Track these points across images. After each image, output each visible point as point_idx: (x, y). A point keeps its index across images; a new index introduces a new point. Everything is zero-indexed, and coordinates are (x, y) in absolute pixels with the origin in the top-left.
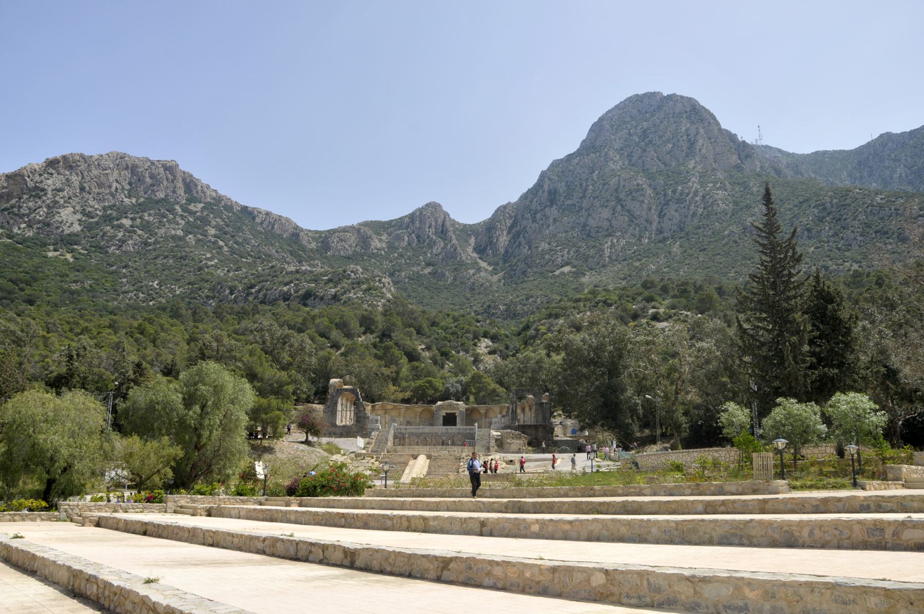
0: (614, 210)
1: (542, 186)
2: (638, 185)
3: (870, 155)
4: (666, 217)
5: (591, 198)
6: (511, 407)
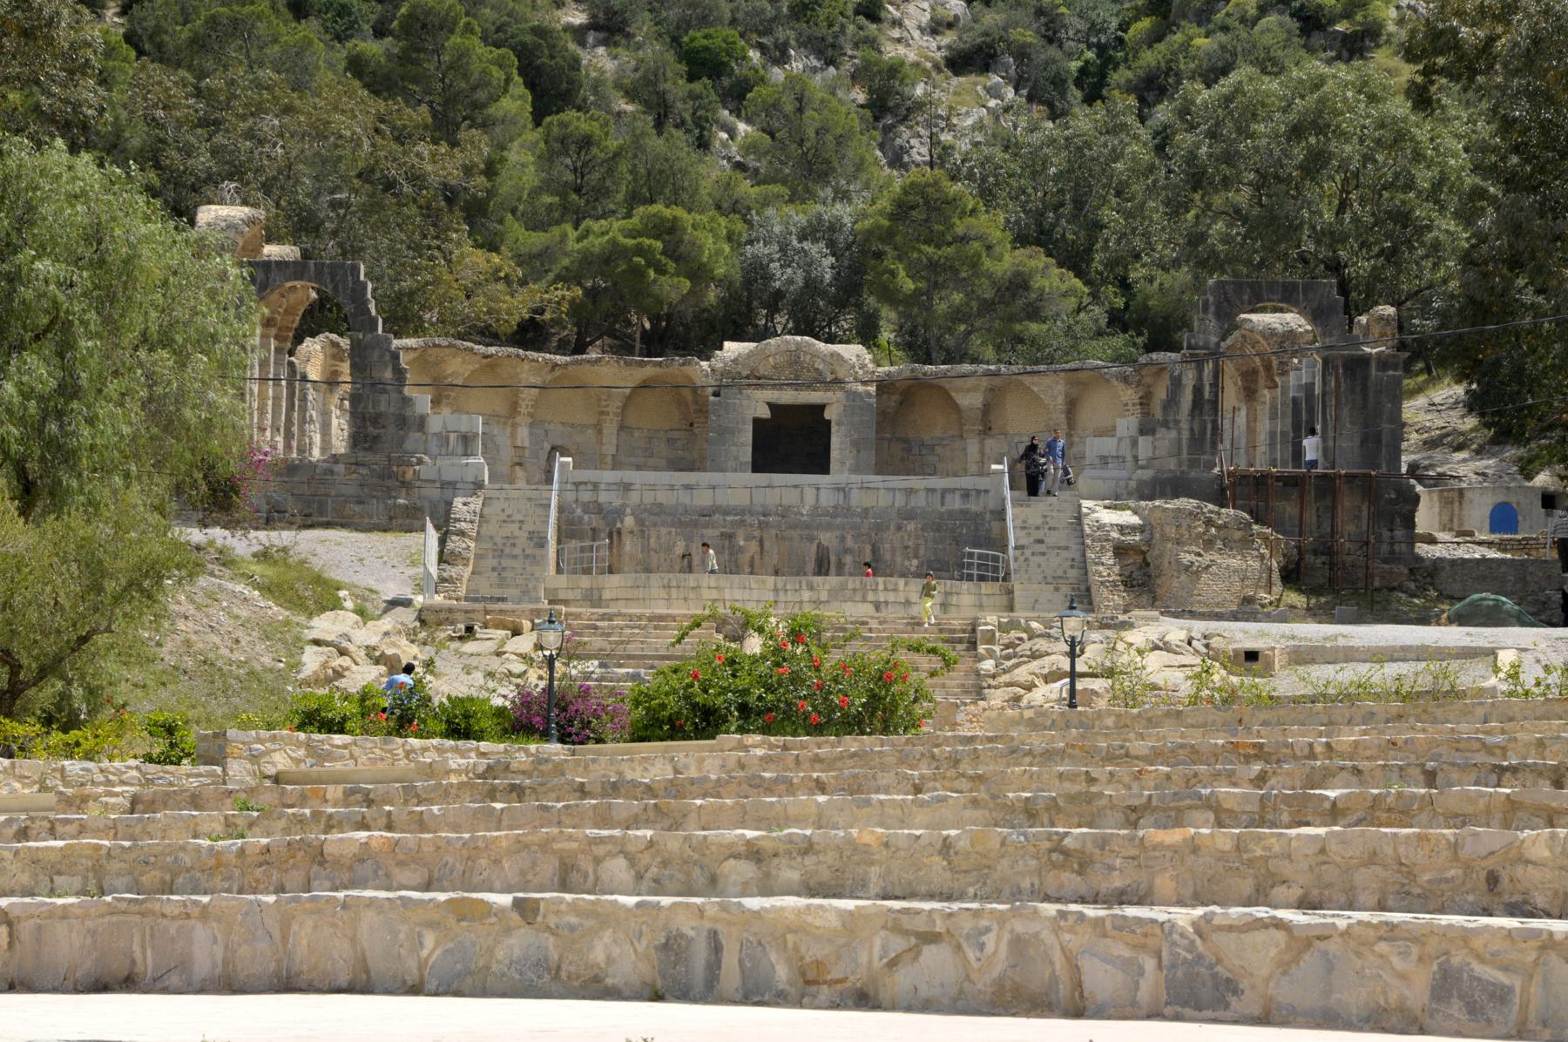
6: (1189, 379)
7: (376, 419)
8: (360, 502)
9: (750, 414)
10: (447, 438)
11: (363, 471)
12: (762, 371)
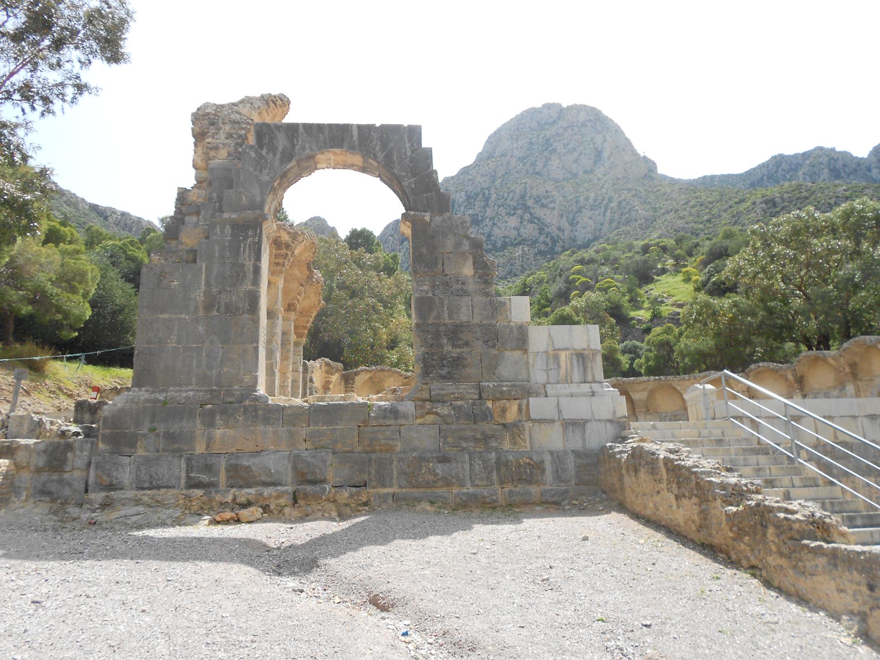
0: (521, 218)
2: (547, 192)
3: (764, 175)
4: (579, 225)
5: (496, 207)
7: (455, 333)
8: (444, 460)
10: (556, 358)
11: (444, 410)
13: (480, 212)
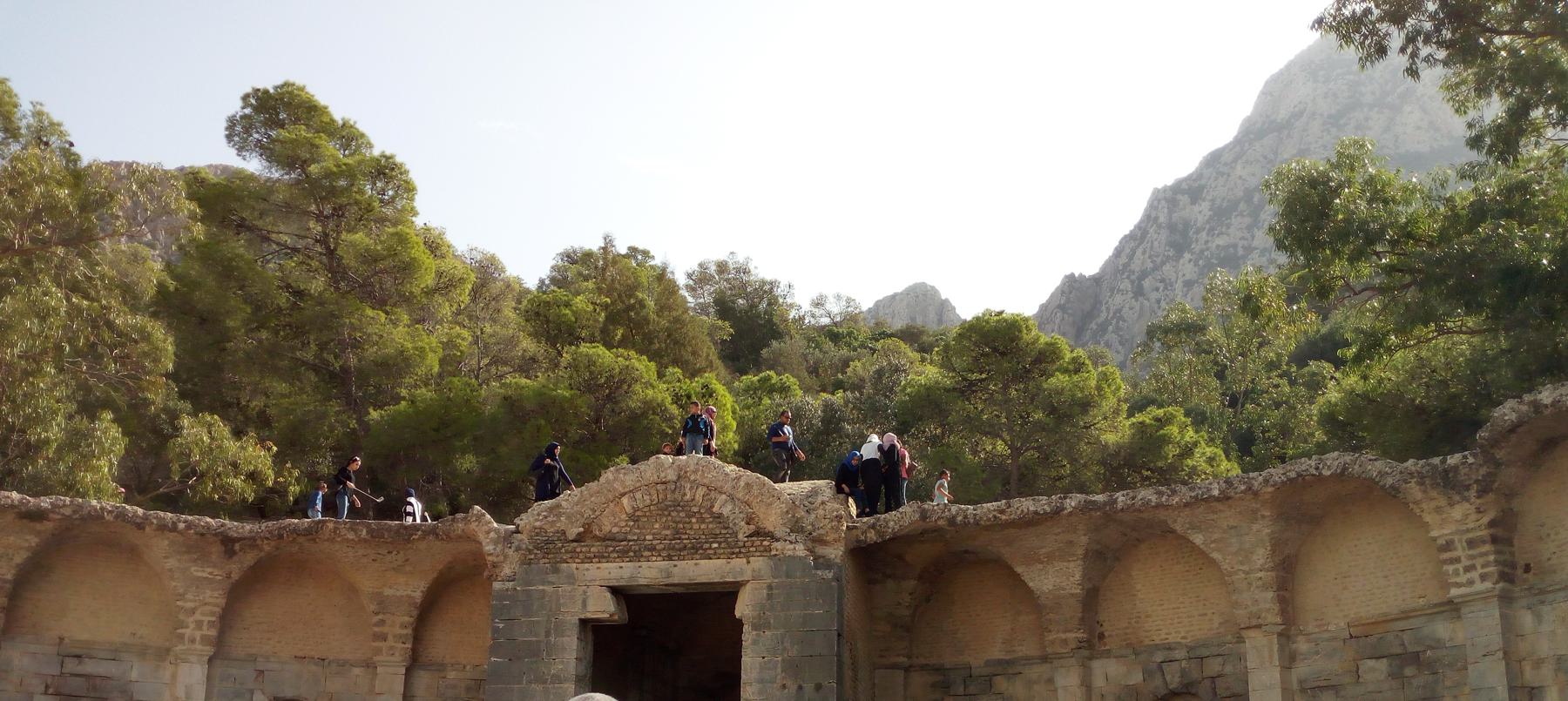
1: (1156, 218)
9: (572, 615)
12: (607, 526)
13: (1243, 238)
